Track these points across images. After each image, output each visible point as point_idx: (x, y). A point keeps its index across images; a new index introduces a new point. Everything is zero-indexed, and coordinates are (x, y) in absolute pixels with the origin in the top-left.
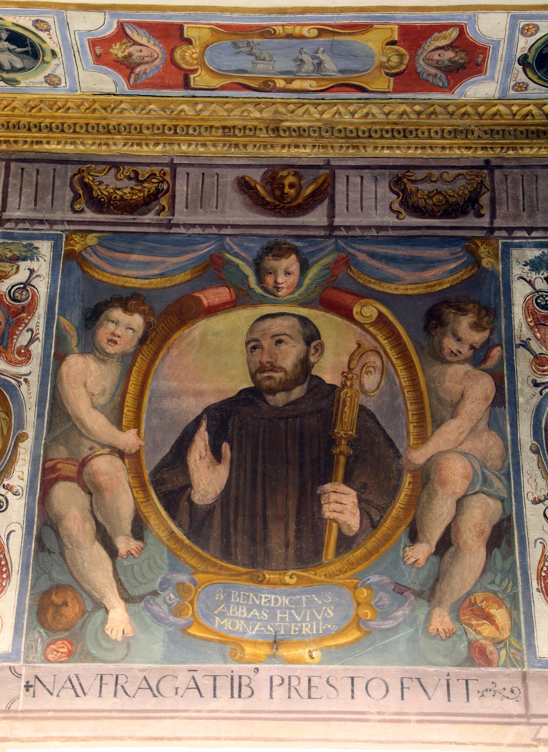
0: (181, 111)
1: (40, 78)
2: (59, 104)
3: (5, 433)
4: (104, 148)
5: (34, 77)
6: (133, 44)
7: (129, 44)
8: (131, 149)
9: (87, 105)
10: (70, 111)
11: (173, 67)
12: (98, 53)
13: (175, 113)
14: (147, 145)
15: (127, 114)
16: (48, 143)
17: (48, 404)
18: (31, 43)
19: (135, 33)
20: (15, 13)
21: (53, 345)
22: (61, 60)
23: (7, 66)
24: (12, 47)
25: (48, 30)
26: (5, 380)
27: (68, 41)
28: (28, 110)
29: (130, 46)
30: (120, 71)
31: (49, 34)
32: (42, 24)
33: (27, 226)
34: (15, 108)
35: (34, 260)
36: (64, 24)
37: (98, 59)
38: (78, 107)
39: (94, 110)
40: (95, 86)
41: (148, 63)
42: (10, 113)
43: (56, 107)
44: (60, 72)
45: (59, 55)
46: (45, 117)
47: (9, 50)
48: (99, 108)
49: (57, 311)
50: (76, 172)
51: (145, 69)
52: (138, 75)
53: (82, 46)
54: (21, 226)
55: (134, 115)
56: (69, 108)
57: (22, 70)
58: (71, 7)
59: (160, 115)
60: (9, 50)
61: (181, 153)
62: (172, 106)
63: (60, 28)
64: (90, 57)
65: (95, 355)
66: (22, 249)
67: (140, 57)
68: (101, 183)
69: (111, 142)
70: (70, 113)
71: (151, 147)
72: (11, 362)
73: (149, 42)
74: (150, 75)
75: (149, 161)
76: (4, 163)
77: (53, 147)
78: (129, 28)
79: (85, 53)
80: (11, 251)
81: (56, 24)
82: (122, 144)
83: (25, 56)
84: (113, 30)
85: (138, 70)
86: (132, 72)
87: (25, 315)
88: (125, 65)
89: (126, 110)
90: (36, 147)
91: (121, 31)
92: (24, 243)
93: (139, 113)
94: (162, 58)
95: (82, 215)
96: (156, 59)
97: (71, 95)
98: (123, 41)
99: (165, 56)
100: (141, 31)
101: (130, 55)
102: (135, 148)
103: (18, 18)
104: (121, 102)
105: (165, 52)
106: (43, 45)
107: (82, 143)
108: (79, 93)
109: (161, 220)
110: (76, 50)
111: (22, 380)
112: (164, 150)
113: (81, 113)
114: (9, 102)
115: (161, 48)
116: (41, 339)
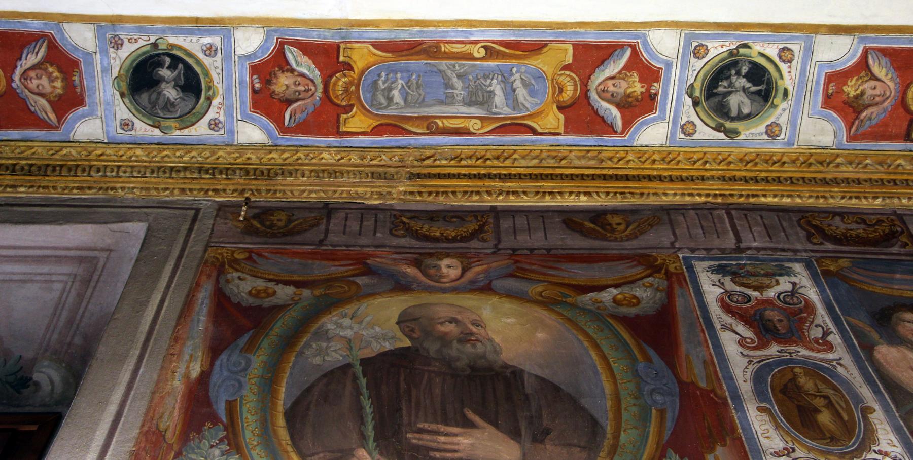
0: (899, 165)
1: (762, 128)
2: (774, 158)
3: (844, 406)
4: (821, 200)
5: (757, 126)
6: (870, 79)
7: (866, 78)
8: (849, 202)
9: (802, 159)
10: (786, 165)
11: (902, 110)
12: (830, 91)
13: (892, 167)
14: (866, 198)
15: (843, 168)
16: (765, 196)
17: (879, 384)
18: (768, 79)
19: (877, 64)
20: (765, 40)
21: (852, 337)
22: (790, 102)
23: (734, 113)
24: (748, 85)
25: (790, 61)
26: (815, 363)
27: (805, 76)
28: (744, 164)
29: (867, 81)
30: (844, 117)
31: (790, 67)
32: (787, 53)
33: (769, 252)
34: (730, 163)
35: (791, 276)
36: (809, 51)
37: (829, 101)
38: (794, 162)
39: (810, 164)
40: (813, 138)
41: (877, 104)
42: (725, 167)
43: (771, 162)
44: (783, 120)
45: (790, 97)
46: (761, 171)
47: (744, 89)
48: (814, 162)
49: (839, 312)
50: (800, 217)
51: (872, 113)
52: (862, 121)
53: (818, 83)
54: (762, 252)
55: (851, 169)
56: (784, 163)
57: (748, 116)
58: (823, 30)
59: (877, 169)
60: (744, 89)
61: (901, 206)
62: (888, 161)
63: (803, 58)
64: (820, 99)
65: (907, 346)
66: (773, 268)
67: (871, 96)
68: (830, 225)
69: (827, 195)
70: (786, 167)
71: (870, 200)
72: (813, 350)
73: (887, 75)
74: (874, 122)
75: (871, 211)
76: (724, 211)
77: (770, 200)
78: (873, 57)
79: (817, 92)
80: (762, 269)
81: (801, 52)
82: (840, 197)
83: (757, 98)
84: (855, 60)
85: (864, 114)
86: (857, 118)
87: (805, 315)
88: (853, 107)
89: (842, 164)
90: (752, 200)
91: (864, 60)
92: (774, 264)
93: (856, 167)
94: (894, 96)
95: (822, 246)
96: (887, 98)
97: (787, 149)
98: (861, 75)
99: (898, 94)
100: (884, 60)
101: (863, 93)
102: (854, 201)
103: (766, 45)
104: (838, 156)
105: (900, 88)
106: (780, 82)
107: (799, 196)
108: (795, 146)
109: (907, 251)
110: (809, 88)
111: (834, 363)
112: (883, 203)
113: (797, 167)
114: (724, 157)
115: (896, 84)
116: (835, 332)
